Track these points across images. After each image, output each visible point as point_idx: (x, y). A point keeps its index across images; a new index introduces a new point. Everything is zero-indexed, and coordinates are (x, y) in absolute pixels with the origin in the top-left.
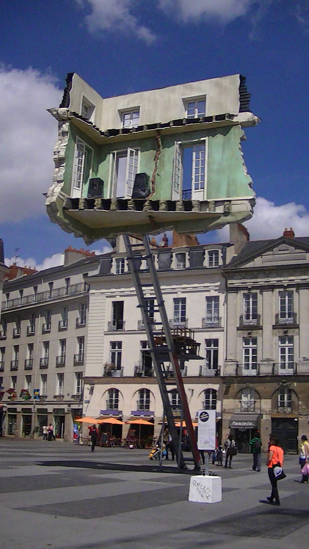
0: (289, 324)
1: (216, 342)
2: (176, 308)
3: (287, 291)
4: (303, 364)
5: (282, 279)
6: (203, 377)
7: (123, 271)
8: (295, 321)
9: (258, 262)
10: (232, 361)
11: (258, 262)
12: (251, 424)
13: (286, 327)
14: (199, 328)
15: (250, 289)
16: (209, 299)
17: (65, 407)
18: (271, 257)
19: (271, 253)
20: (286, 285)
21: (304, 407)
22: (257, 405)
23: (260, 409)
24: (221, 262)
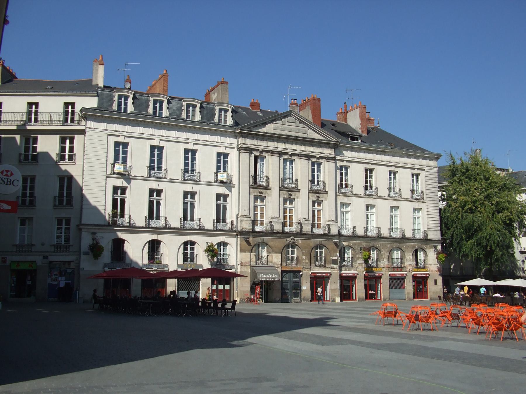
0: (293, 188)
2: (116, 152)
3: (289, 159)
6: (383, 238)
7: (125, 109)
8: (297, 185)
9: (269, 128)
11: (269, 128)
12: (276, 276)
13: (289, 190)
14: (210, 182)
15: (318, 158)
16: (219, 155)
17: (39, 259)
21: (307, 261)
22: (270, 258)
23: (272, 262)
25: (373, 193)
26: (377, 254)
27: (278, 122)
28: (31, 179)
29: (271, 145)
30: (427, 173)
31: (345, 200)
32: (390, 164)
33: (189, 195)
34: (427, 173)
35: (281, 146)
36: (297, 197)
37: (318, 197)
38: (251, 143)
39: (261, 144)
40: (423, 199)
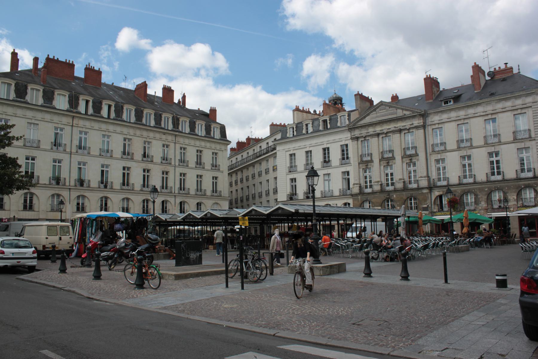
1: (348, 173)
4: (399, 183)
5: (383, 128)
9: (367, 120)
10: (357, 184)
11: (367, 120)
18: (375, 115)
19: (375, 112)
20: (385, 132)
24: (347, 123)
25: (129, 188)
26: (475, 199)
27: (374, 113)
28: (26, 209)
29: (371, 130)
30: (534, 109)
31: (439, 157)
32: (484, 114)
33: (293, 180)
34: (534, 109)
35: (378, 129)
36: (394, 163)
37: (411, 160)
38: (357, 133)
39: (364, 132)
40: (530, 137)
